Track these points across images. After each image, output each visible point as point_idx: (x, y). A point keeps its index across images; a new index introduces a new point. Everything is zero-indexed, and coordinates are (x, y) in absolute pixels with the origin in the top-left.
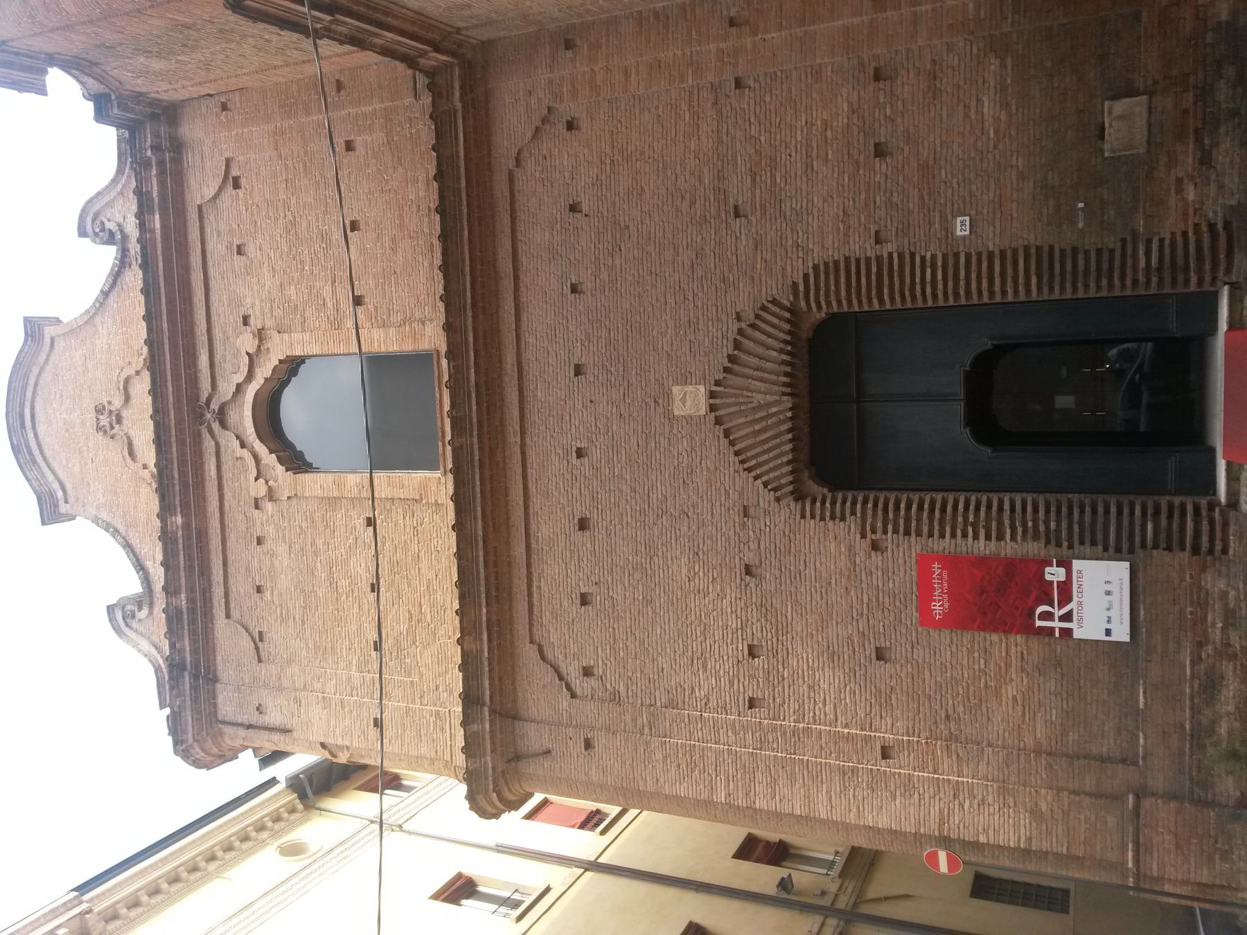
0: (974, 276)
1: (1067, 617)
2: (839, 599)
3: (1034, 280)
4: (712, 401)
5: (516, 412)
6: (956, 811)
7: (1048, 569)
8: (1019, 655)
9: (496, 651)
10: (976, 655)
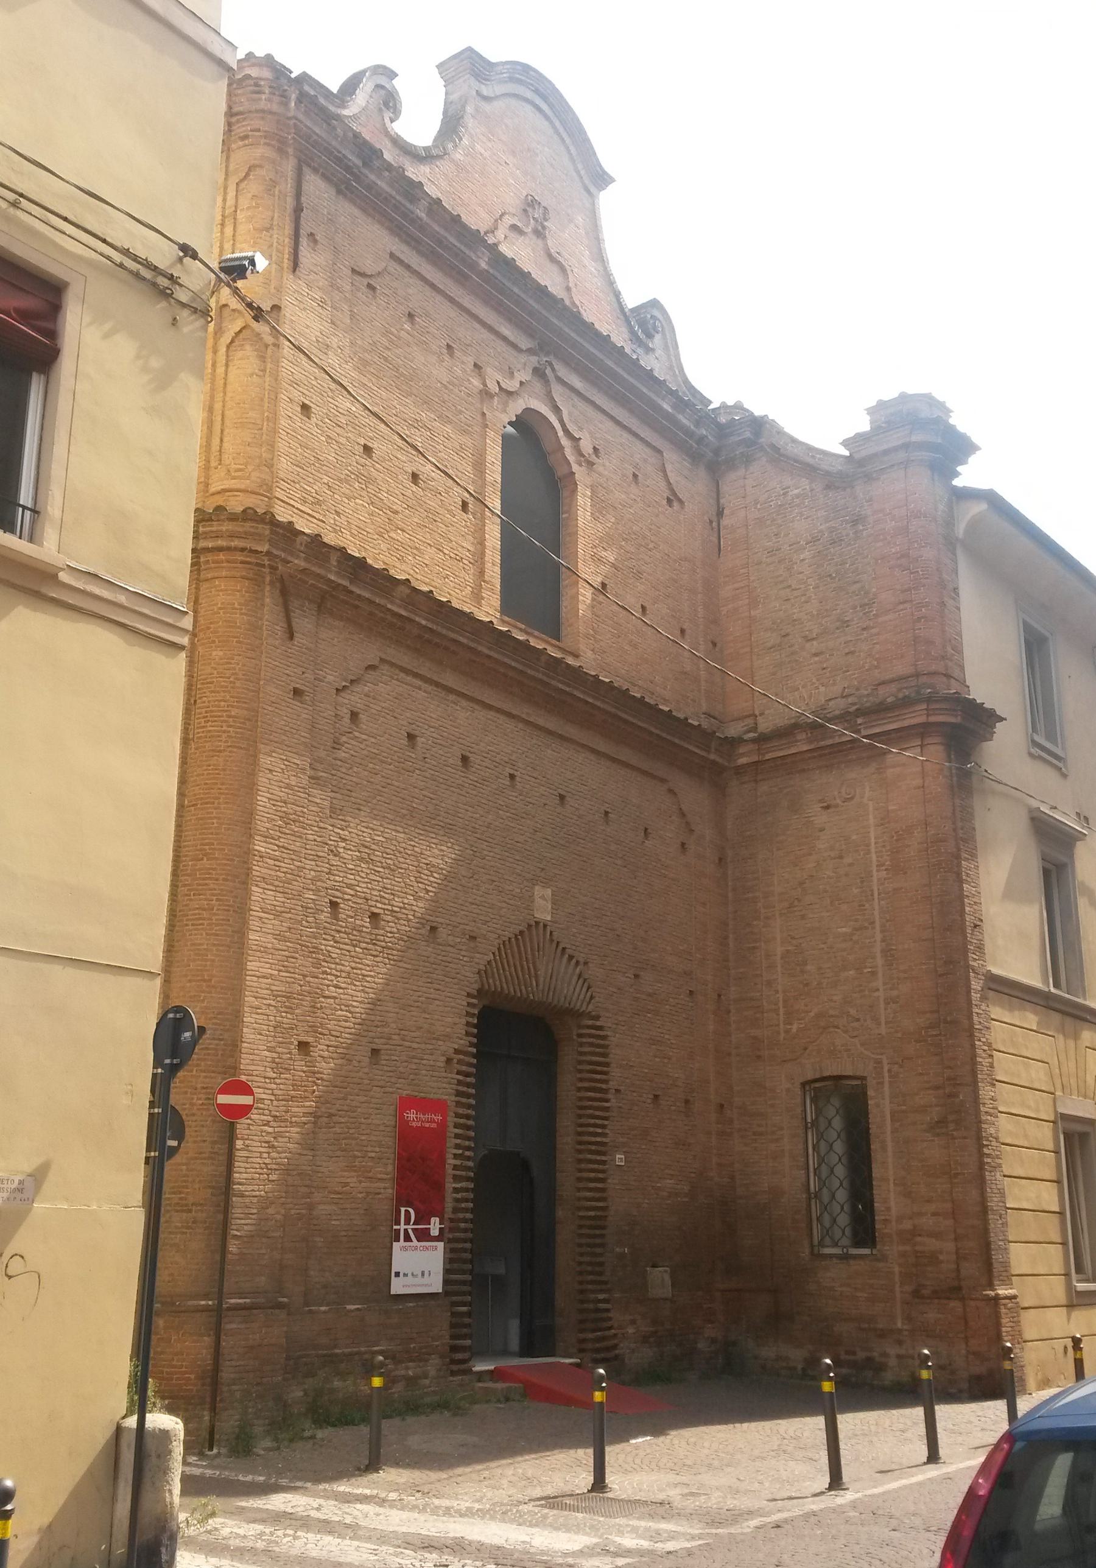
0: (596, 1166)
1: (408, 1238)
2: (414, 1019)
3: (592, 1213)
4: (542, 924)
5: (541, 722)
6: (263, 1117)
7: (437, 1219)
8: (378, 1191)
9: (382, 615)
10: (377, 1149)
